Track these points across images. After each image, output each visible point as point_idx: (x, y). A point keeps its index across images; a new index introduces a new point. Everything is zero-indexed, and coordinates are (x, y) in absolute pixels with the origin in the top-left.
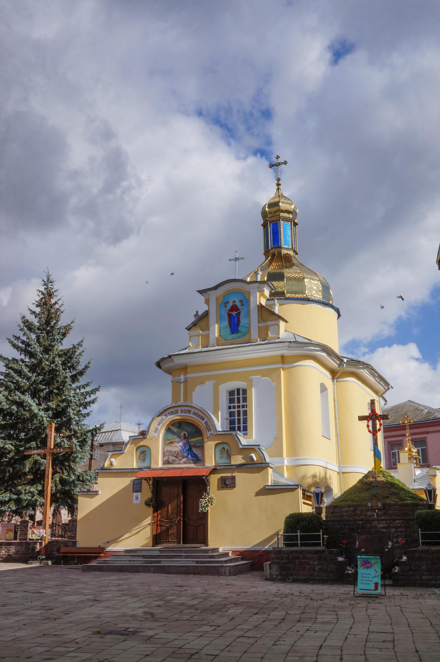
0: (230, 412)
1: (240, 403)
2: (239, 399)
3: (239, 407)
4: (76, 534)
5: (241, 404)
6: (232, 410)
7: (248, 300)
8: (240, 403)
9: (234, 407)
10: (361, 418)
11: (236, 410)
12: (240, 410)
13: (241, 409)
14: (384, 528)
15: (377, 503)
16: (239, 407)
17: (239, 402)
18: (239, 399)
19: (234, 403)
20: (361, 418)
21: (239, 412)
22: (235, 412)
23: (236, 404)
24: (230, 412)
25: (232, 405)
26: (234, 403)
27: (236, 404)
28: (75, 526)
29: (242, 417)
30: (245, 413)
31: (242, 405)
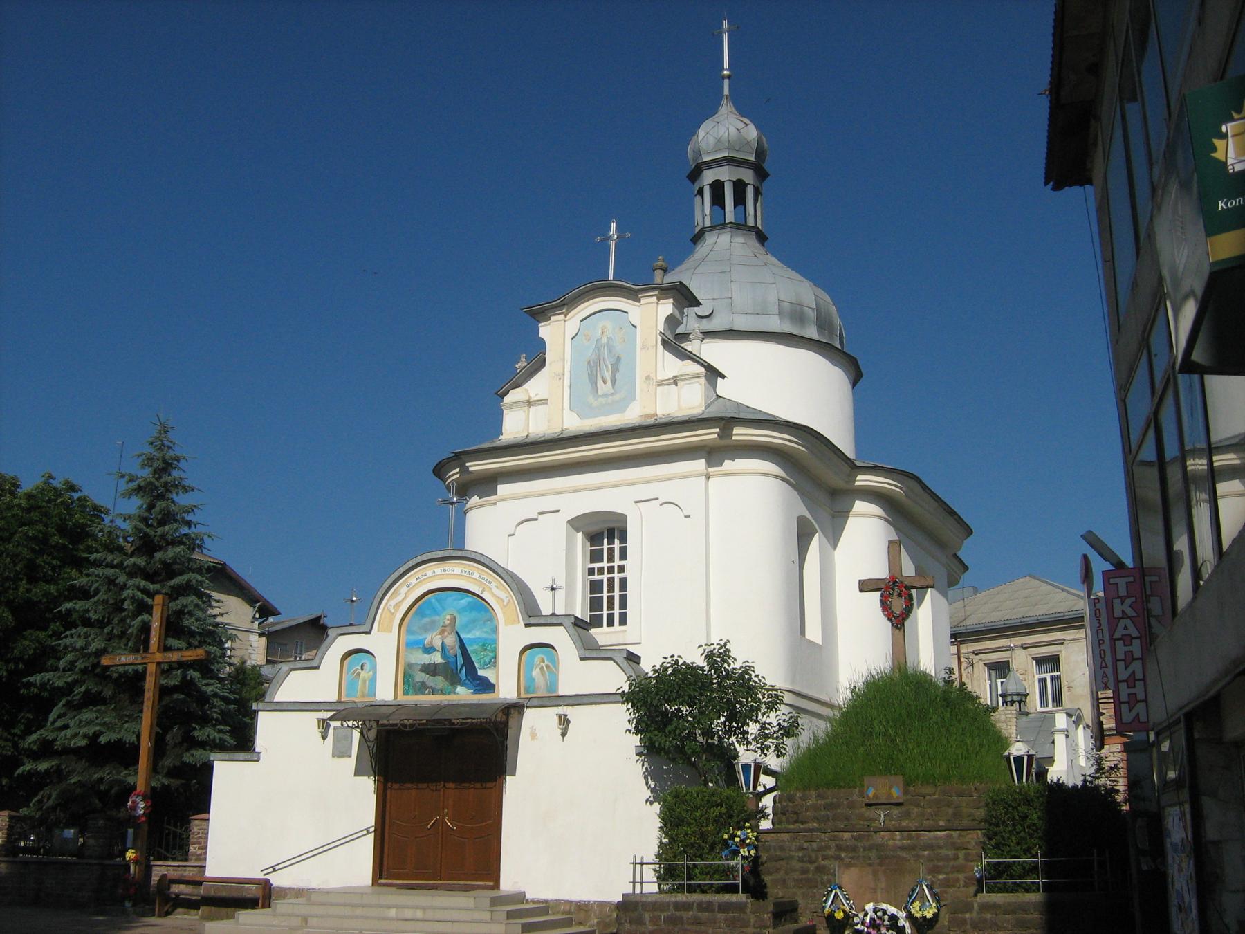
0: (592, 582)
1: (614, 562)
2: (611, 551)
3: (611, 570)
4: (206, 848)
5: (617, 562)
6: (596, 577)
7: (635, 327)
8: (614, 562)
9: (601, 571)
10: (865, 586)
11: (605, 577)
12: (613, 578)
13: (617, 576)
14: (903, 848)
15: (890, 788)
16: (611, 570)
17: (611, 559)
18: (611, 551)
19: (602, 561)
20: (865, 586)
21: (611, 581)
22: (602, 581)
23: (605, 564)
24: (592, 582)
25: (596, 565)
26: (602, 561)
27: (605, 564)
28: (206, 831)
29: (617, 594)
30: (623, 582)
31: (619, 566)
